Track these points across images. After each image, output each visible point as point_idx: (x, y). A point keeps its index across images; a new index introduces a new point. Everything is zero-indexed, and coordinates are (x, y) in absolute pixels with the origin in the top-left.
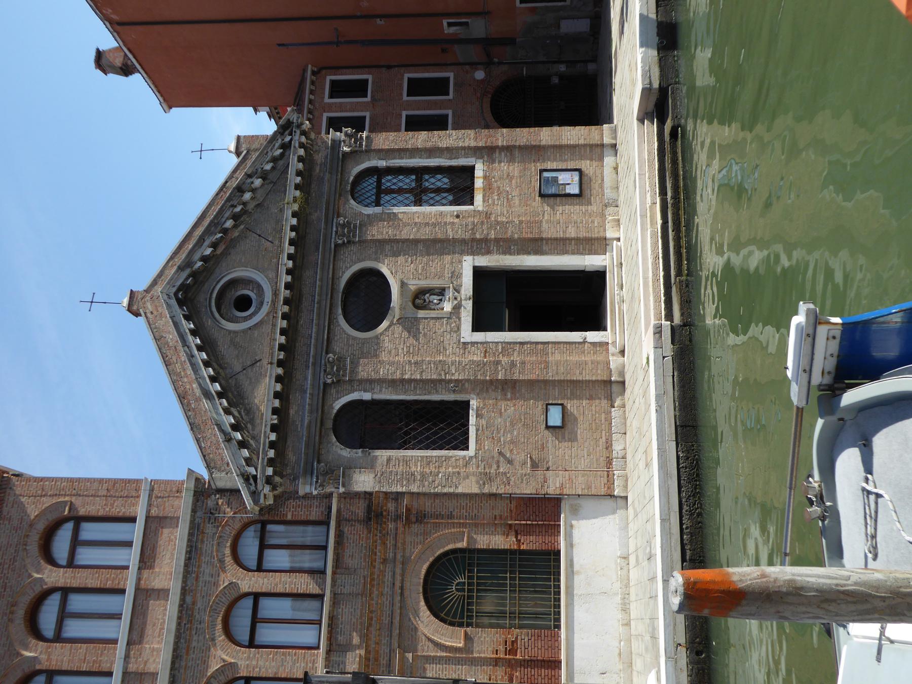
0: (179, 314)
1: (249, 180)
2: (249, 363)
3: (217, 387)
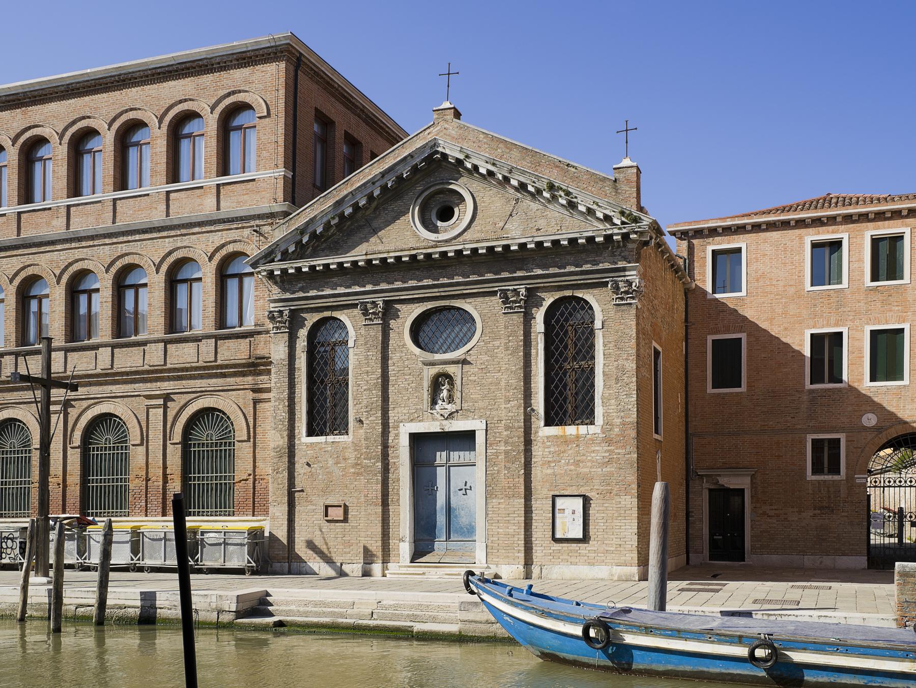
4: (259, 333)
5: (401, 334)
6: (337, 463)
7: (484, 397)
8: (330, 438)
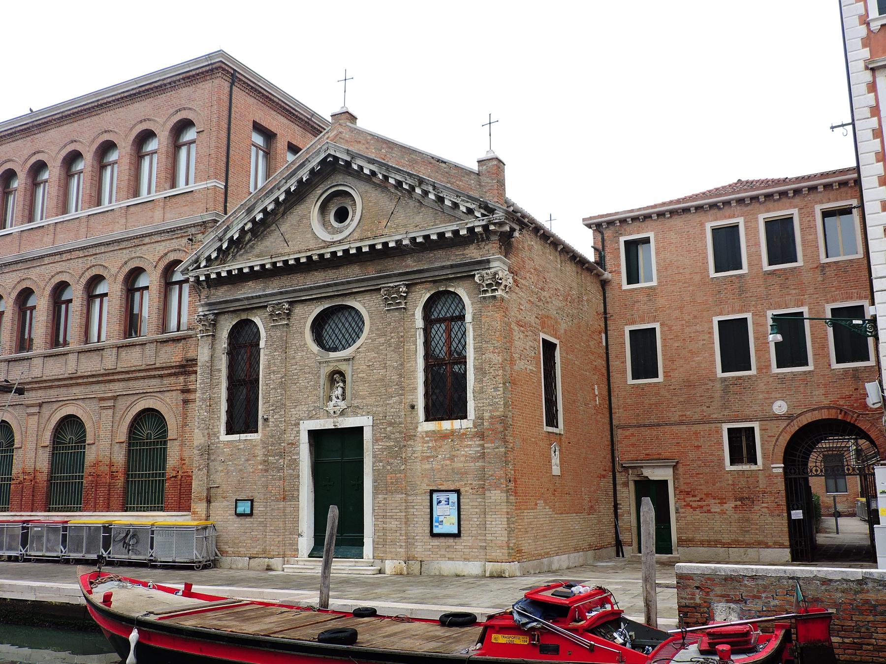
0: (314, 163)
1: (430, 189)
2: (286, 237)
3: (259, 217)
4: (190, 337)
5: (302, 333)
6: (248, 460)
8: (243, 436)
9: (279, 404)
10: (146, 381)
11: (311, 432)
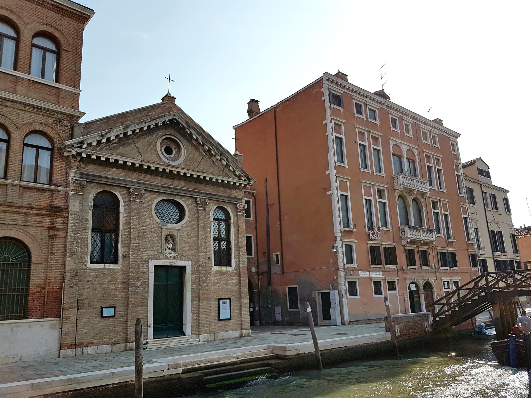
2: (140, 151)
7: (190, 250)
9: (137, 248)
10: (8, 215)
11: (156, 267)
